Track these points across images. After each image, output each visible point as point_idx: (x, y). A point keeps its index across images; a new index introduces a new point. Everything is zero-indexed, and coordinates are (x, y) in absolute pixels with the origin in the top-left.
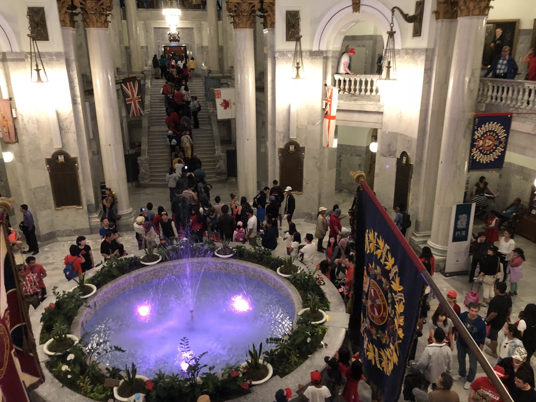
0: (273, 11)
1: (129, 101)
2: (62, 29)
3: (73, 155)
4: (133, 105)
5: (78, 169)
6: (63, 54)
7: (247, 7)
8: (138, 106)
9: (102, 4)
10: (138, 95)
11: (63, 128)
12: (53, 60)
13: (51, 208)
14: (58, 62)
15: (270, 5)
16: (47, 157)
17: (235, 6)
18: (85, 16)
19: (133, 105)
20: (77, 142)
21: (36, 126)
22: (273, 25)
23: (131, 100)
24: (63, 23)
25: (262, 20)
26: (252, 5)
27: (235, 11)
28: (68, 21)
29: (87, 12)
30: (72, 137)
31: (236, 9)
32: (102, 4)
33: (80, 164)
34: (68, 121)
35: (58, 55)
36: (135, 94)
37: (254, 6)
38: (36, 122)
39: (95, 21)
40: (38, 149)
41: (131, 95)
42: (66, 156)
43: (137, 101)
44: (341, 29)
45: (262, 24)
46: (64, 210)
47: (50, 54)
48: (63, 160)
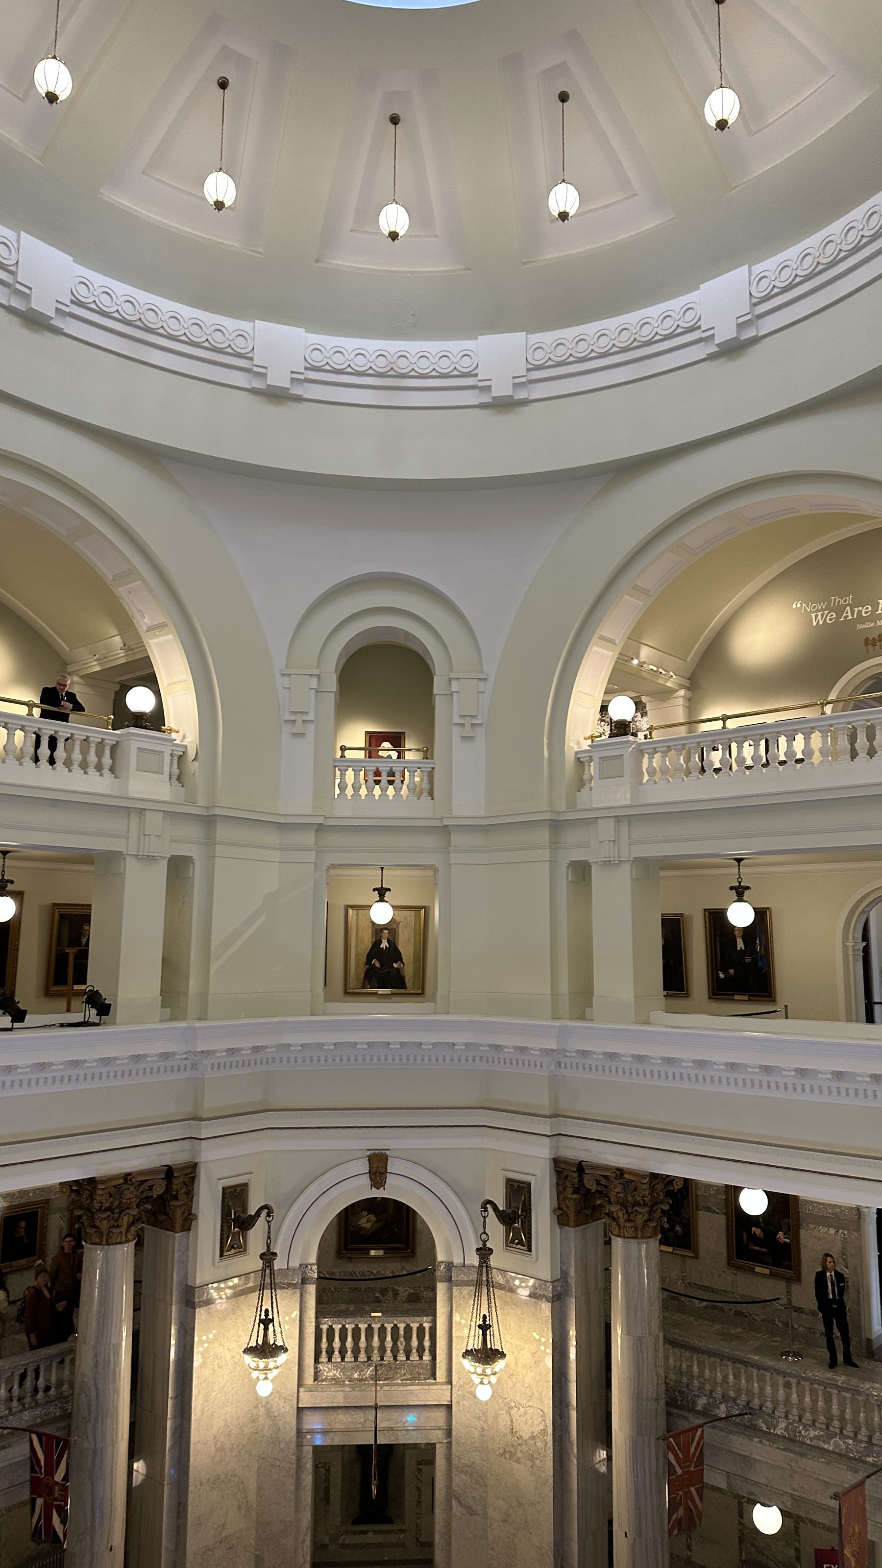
24: (561, 1217)
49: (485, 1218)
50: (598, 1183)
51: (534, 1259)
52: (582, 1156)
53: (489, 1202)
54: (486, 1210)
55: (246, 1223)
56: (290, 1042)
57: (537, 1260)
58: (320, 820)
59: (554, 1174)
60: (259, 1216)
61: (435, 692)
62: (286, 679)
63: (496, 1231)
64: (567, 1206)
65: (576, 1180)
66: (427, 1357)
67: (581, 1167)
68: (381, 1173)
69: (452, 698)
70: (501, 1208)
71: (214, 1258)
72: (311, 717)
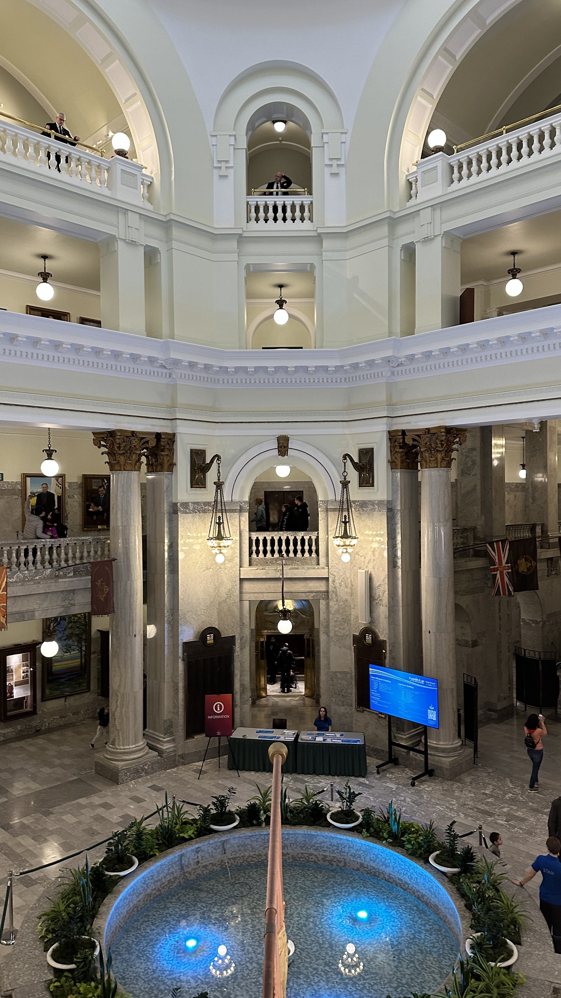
1: (495, 570)
2: (392, 472)
3: (382, 637)
4: (498, 576)
5: (385, 658)
6: (386, 503)
8: (506, 579)
10: (506, 563)
11: (376, 598)
12: (373, 510)
13: (352, 706)
14: (380, 513)
16: (356, 634)
19: (498, 576)
20: (387, 620)
21: (348, 590)
23: (497, 570)
24: (393, 464)
28: (398, 462)
30: (382, 611)
33: (388, 652)
34: (382, 588)
35: (380, 503)
36: (504, 561)
38: (350, 586)
40: (346, 620)
41: (497, 561)
42: (375, 636)
43: (505, 571)
46: (365, 713)
47: (372, 503)
48: (370, 642)
49: (345, 463)
50: (414, 440)
51: (376, 491)
52: (404, 427)
53: (347, 455)
54: (346, 459)
55: (206, 468)
56: (228, 366)
57: (378, 490)
58: (240, 232)
59: (388, 440)
60: (213, 462)
61: (312, 145)
62: (214, 139)
63: (353, 475)
64: (396, 458)
65: (401, 441)
66: (314, 555)
67: (404, 432)
68: (285, 447)
69: (324, 151)
70: (356, 460)
71: (187, 489)
72: (231, 164)
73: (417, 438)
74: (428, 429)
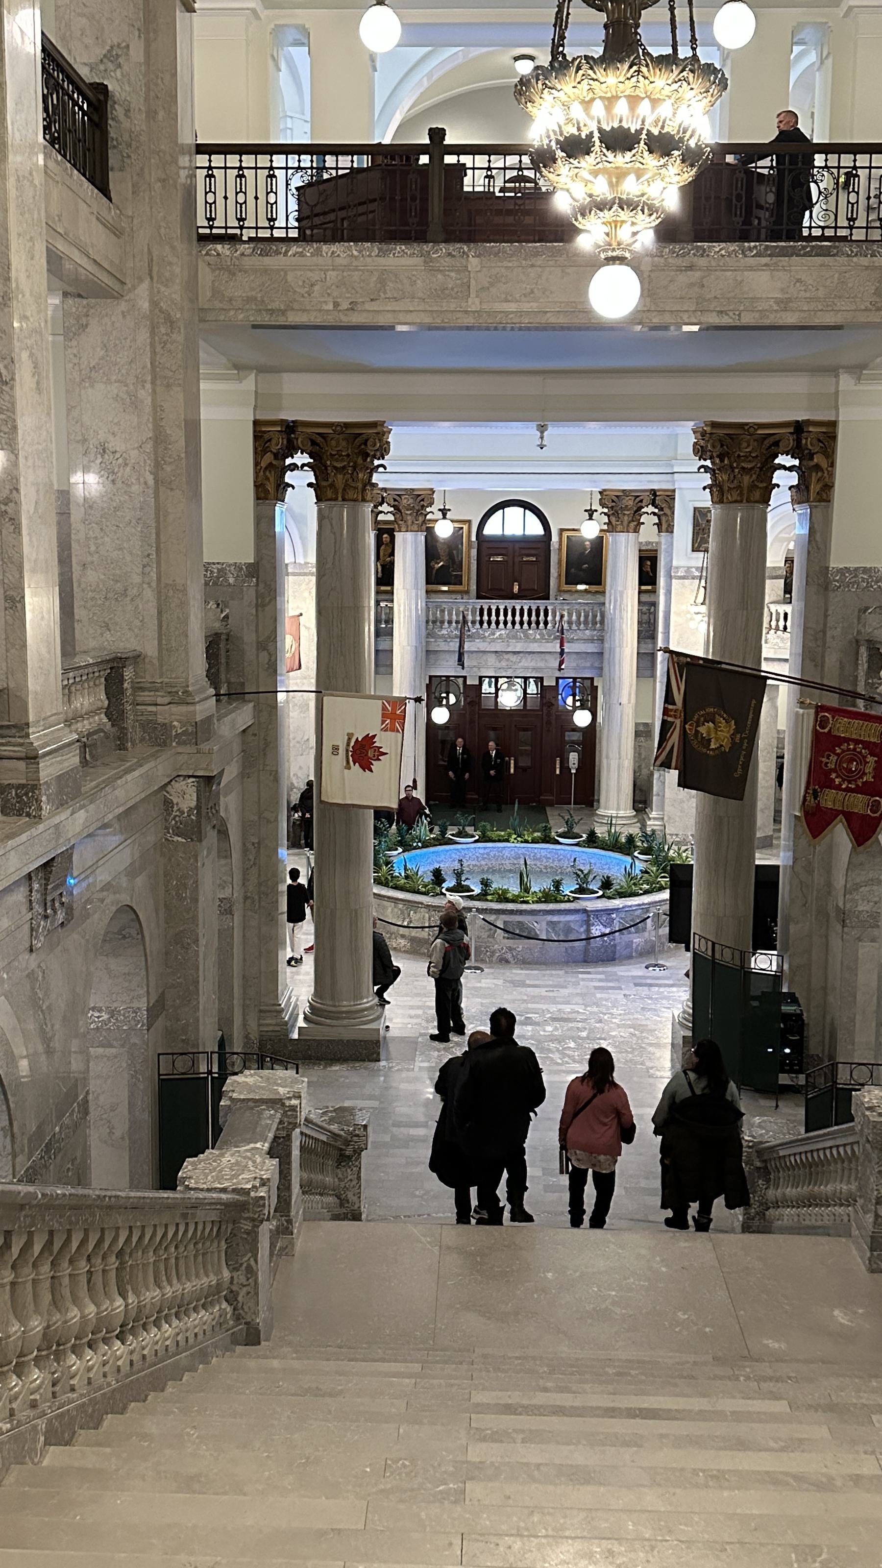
0: (672, 508)
7: (631, 503)
9: (423, 500)
15: (668, 499)
17: (613, 501)
18: (398, 516)
22: (670, 530)
25: (656, 520)
26: (638, 499)
27: (612, 507)
29: (400, 511)
31: (614, 504)
32: (423, 500)
37: (641, 501)
39: (410, 522)
44: (780, 532)
45: (656, 526)
73: (398, 498)
74: (413, 490)
